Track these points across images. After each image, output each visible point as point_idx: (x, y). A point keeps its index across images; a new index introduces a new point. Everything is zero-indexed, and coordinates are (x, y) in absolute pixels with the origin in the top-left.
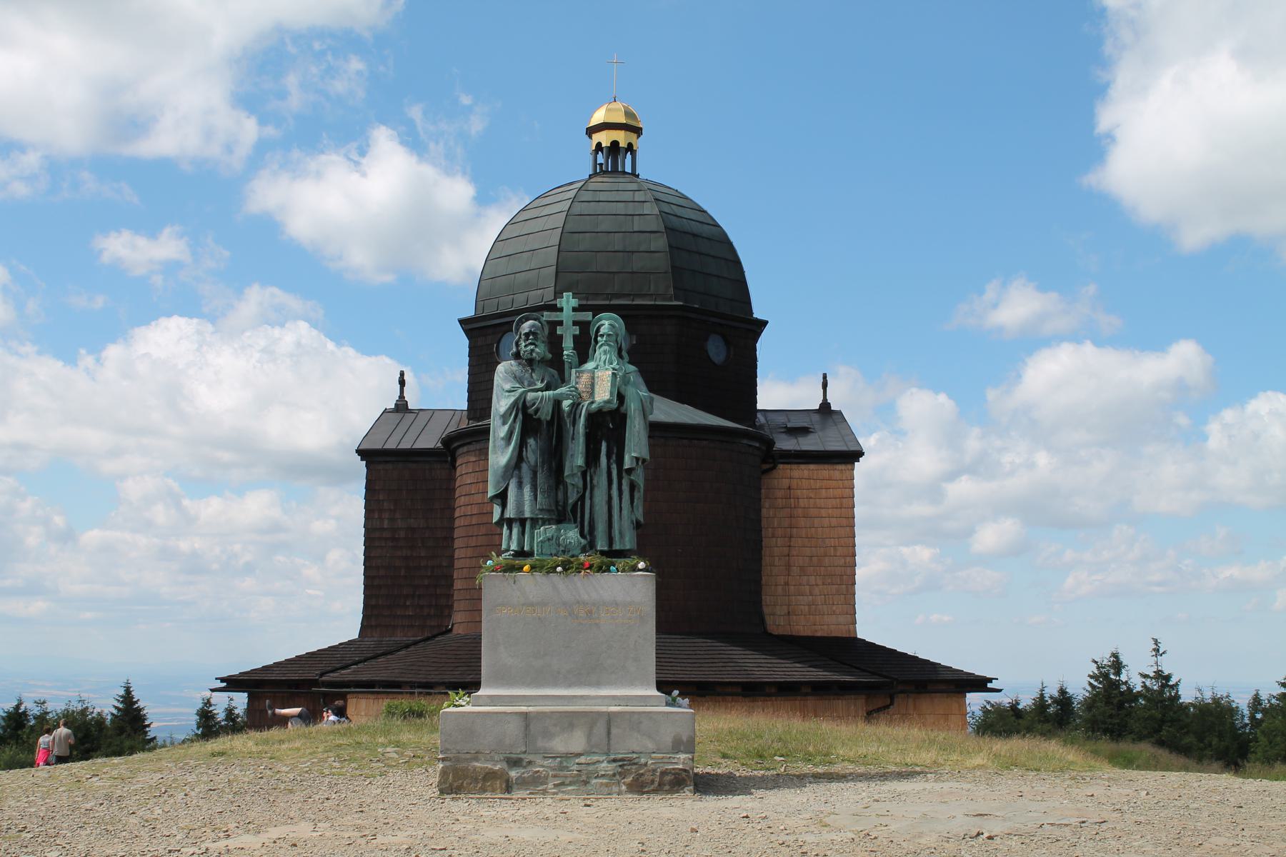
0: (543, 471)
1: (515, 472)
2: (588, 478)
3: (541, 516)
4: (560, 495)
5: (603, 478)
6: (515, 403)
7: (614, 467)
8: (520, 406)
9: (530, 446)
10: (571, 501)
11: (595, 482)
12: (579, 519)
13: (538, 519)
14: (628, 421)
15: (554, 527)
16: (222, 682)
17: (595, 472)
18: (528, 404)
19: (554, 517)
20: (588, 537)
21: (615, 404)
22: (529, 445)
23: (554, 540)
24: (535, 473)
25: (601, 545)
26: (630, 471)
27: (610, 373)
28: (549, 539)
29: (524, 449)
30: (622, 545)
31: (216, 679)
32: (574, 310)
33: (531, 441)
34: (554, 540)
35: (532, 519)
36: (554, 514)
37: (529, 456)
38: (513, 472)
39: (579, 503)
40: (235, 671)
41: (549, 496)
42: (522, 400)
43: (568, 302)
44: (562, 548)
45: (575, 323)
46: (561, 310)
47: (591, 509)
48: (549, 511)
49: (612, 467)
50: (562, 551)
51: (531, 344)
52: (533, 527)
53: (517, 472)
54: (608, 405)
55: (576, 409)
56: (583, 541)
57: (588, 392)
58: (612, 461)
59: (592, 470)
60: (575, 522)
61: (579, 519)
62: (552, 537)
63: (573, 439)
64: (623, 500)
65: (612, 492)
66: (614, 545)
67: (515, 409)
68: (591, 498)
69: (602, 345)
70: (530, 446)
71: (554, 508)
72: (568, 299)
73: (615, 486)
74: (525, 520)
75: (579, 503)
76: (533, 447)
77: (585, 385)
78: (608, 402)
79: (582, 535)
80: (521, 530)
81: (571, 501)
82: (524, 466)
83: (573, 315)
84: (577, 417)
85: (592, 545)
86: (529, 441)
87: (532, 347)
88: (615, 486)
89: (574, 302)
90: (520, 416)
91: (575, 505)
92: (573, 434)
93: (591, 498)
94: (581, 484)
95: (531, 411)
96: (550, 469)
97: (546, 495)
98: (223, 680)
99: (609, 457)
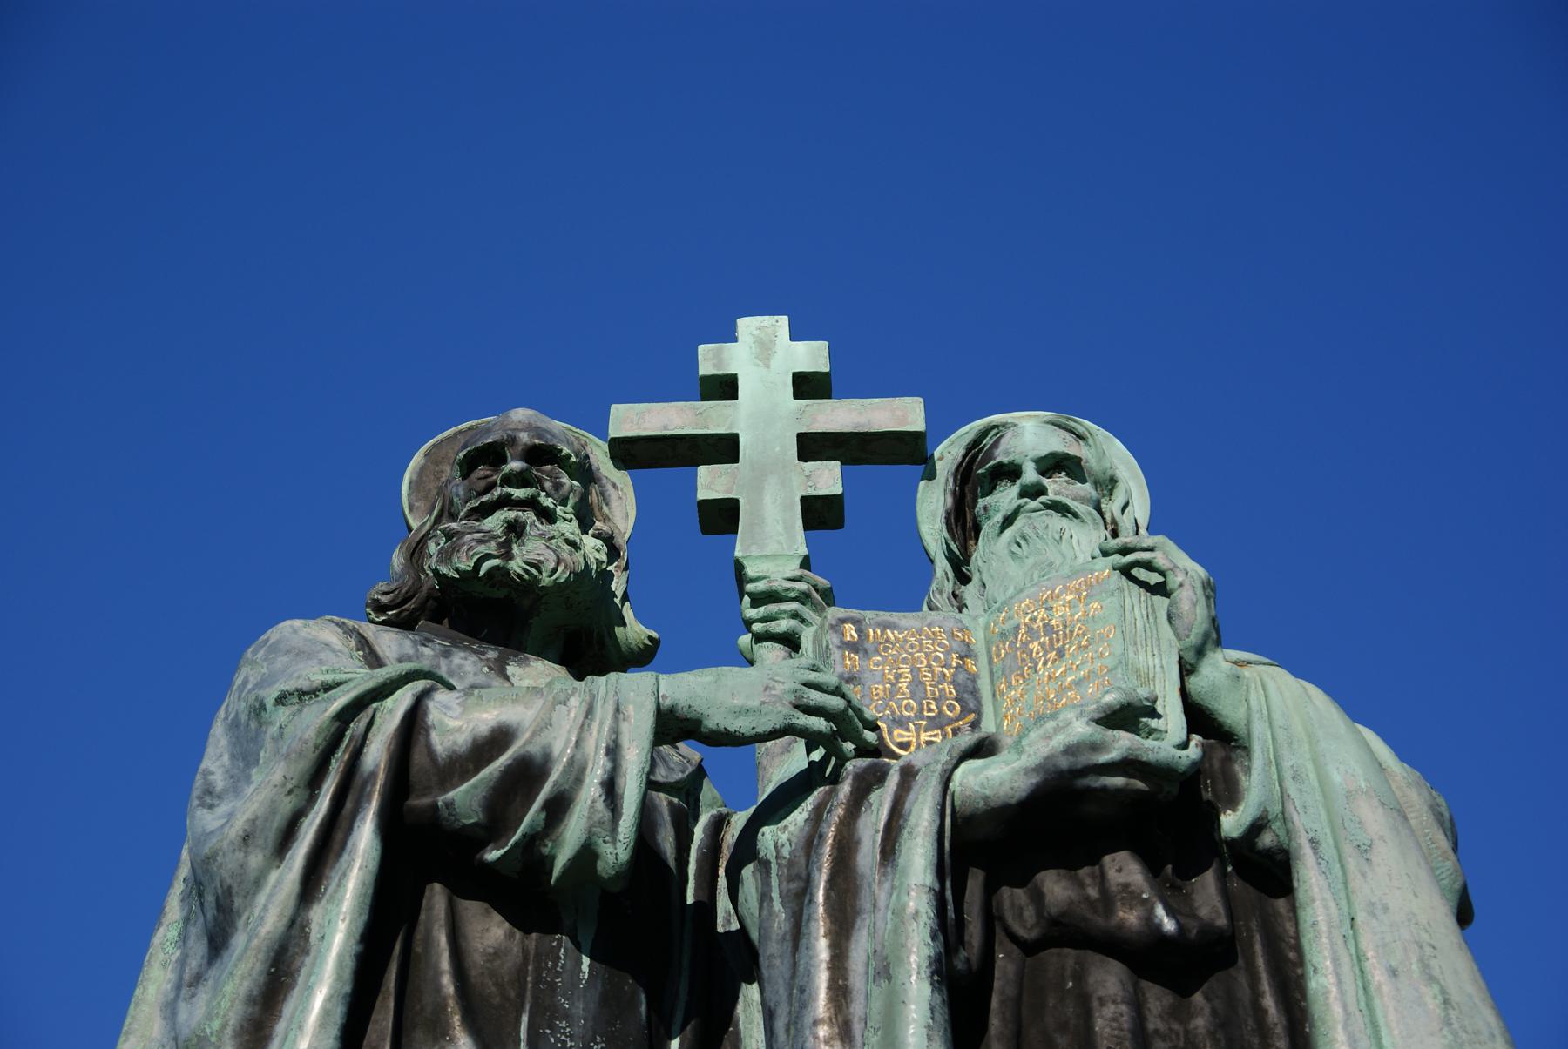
8: (376, 754)
32: (807, 386)
43: (765, 350)
45: (812, 446)
51: (506, 502)
54: (1121, 743)
69: (1008, 521)
72: (765, 350)
89: (813, 356)
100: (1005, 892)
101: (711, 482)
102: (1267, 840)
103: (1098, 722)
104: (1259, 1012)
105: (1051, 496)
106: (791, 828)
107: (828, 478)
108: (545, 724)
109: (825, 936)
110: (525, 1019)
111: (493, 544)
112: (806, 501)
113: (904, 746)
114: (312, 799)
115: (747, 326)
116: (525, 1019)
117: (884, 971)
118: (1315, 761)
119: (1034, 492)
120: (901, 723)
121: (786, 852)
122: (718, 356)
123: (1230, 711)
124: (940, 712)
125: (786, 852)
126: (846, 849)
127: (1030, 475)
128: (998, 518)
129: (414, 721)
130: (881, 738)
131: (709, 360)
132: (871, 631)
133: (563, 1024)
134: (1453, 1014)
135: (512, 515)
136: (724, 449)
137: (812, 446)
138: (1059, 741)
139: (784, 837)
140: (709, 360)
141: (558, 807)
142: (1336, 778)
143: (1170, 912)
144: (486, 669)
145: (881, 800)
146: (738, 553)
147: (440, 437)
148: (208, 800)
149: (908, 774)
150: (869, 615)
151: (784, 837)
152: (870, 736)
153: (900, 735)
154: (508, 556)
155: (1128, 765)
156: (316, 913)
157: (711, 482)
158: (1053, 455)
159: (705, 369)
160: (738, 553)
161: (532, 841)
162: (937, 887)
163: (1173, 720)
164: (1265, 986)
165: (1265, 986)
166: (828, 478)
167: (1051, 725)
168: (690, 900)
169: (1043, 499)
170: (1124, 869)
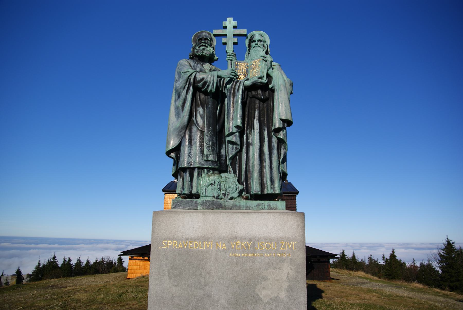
0: (209, 131)
3: (206, 166)
8: (192, 80)
13: (203, 168)
14: (276, 93)
16: (121, 253)
17: (250, 133)
22: (198, 112)
24: (202, 132)
25: (255, 188)
26: (278, 130)
28: (212, 184)
30: (272, 190)
31: (120, 252)
32: (234, 27)
33: (200, 110)
35: (199, 168)
36: (217, 165)
37: (198, 120)
39: (238, 157)
40: (125, 250)
41: (213, 150)
43: (230, 22)
44: (222, 192)
45: (235, 35)
46: (225, 27)
48: (212, 161)
50: (223, 194)
51: (203, 45)
52: (199, 175)
54: (260, 80)
56: (241, 187)
62: (215, 182)
66: (266, 190)
67: (188, 83)
70: (199, 113)
72: (230, 22)
74: (194, 169)
75: (238, 157)
76: (201, 112)
79: (239, 181)
82: (194, 129)
83: (234, 31)
85: (247, 189)
86: (198, 109)
87: (204, 47)
89: (235, 23)
90: (191, 89)
91: (233, 158)
94: (239, 143)
95: (200, 85)
96: (214, 130)
98: (122, 252)
100: (249, 93)
101: (224, 40)
102: (273, 88)
104: (270, 104)
107: (236, 40)
108: (207, 78)
110: (206, 105)
112: (234, 43)
113: (241, 77)
114: (186, 84)
115: (228, 19)
116: (206, 105)
117: (237, 102)
118: (278, 81)
119: (257, 44)
120: (240, 75)
121: (229, 88)
122: (225, 23)
123: (271, 75)
125: (229, 88)
126: (234, 89)
128: (253, 47)
129: (195, 77)
130: (238, 77)
131: (224, 24)
134: (286, 107)
136: (225, 35)
137: (235, 35)
138: (254, 80)
139: (229, 87)
140: (224, 24)
141: (208, 86)
142: (280, 83)
143: (263, 96)
145: (238, 84)
146: (226, 50)
147: (196, 34)
148: (176, 82)
149: (240, 82)
150: (238, 61)
151: (229, 87)
152: (237, 77)
153: (241, 76)
154: (203, 52)
155: (260, 83)
156: (187, 96)
157: (224, 40)
158: (259, 40)
159: (223, 25)
160: (226, 50)
161: (206, 89)
164: (271, 102)
165: (271, 102)
166: (236, 40)
167: (253, 78)
168: (221, 90)
169: (258, 45)
170: (260, 92)
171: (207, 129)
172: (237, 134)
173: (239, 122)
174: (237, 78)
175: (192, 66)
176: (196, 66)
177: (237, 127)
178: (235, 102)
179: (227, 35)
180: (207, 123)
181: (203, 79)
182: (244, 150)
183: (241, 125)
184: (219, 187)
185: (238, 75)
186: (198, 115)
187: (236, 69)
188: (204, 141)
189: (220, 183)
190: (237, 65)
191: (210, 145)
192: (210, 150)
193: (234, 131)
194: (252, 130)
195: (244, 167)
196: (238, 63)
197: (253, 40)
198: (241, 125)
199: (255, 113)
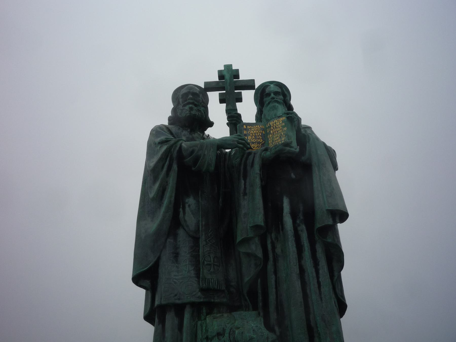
1: (169, 240)
2: (269, 247)
4: (232, 274)
5: (290, 244)
6: (167, 153)
7: (303, 227)
8: (175, 154)
9: (189, 206)
10: (246, 279)
11: (278, 250)
12: (260, 304)
14: (315, 170)
15: (225, 315)
18: (185, 153)
19: (225, 300)
20: (277, 329)
21: (295, 148)
22: (187, 206)
23: (227, 335)
24: (196, 240)
27: (284, 118)
28: (219, 334)
29: (181, 210)
33: (191, 201)
34: (227, 335)
35: (193, 304)
37: (187, 218)
38: (166, 241)
39: (259, 281)
42: (177, 148)
47: (276, 288)
49: (299, 228)
53: (172, 241)
55: (247, 159)
57: (259, 143)
58: (298, 222)
59: (273, 235)
60: (255, 308)
61: (260, 304)
63: (245, 194)
64: (321, 272)
65: (303, 262)
67: (168, 159)
68: (275, 273)
69: (269, 103)
70: (189, 206)
71: (224, 288)
73: (307, 253)
75: (259, 281)
77: (255, 136)
78: (287, 145)
80: (176, 321)
81: (246, 279)
84: (248, 168)
86: (187, 200)
88: (307, 253)
90: (175, 167)
92: (245, 188)
93: (275, 273)
94: (260, 254)
97: (212, 270)
99: (294, 215)
103: (284, 146)
105: (275, 99)
106: (237, 162)
109: (243, 180)
111: (188, 112)
113: (254, 147)
116: (200, 193)
119: (273, 98)
120: (253, 143)
124: (259, 141)
127: (272, 95)
128: (267, 103)
132: (248, 126)
133: (205, 194)
135: (191, 106)
142: (319, 153)
144: (189, 134)
145: (251, 157)
149: (255, 154)
152: (248, 146)
158: (276, 91)
162: (260, 173)
163: (294, 144)
169: (274, 100)
171: (203, 233)
172: (257, 240)
173: (260, 219)
174: (248, 149)
175: (174, 134)
176: (181, 134)
177: (256, 227)
178: (248, 186)
179: (226, 88)
180: (204, 223)
181: (192, 152)
182: (270, 266)
183: (262, 224)
184: (232, 339)
185: (249, 144)
186: (187, 209)
187: (245, 135)
188: (199, 255)
189: (234, 332)
190: (245, 129)
191: (211, 261)
192: (210, 271)
193: (251, 235)
194: (281, 232)
195: (272, 298)
196: (247, 127)
197: (266, 93)
198: (262, 224)
199: (282, 203)
